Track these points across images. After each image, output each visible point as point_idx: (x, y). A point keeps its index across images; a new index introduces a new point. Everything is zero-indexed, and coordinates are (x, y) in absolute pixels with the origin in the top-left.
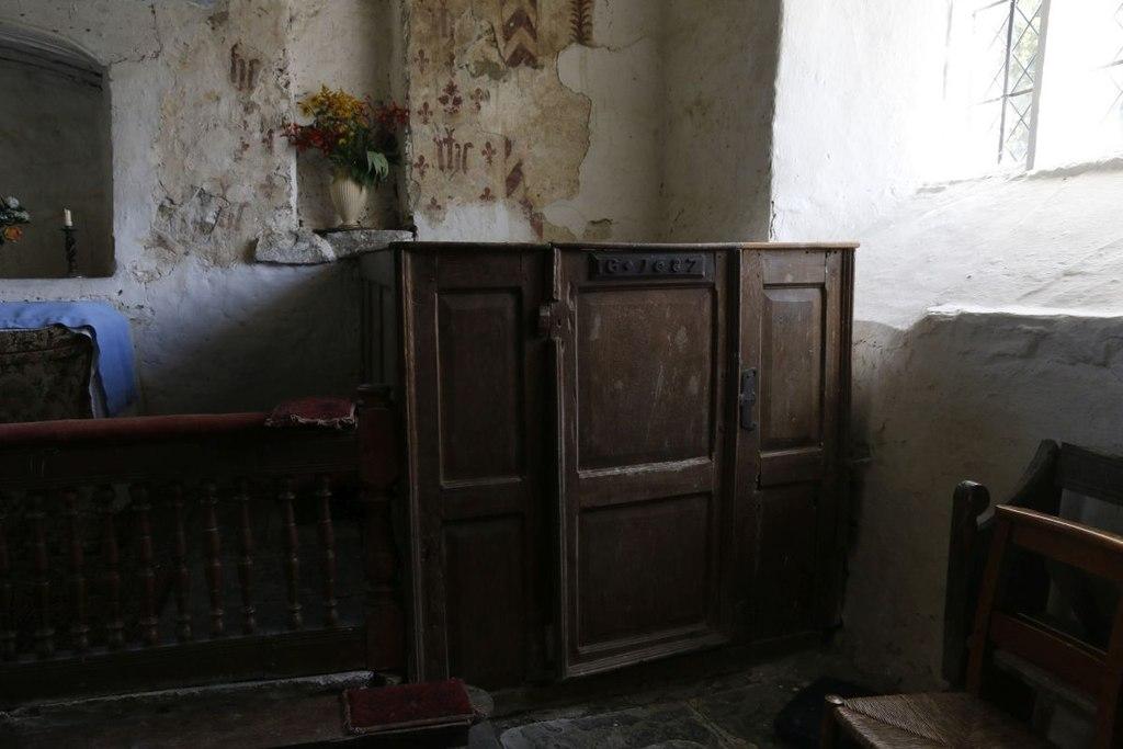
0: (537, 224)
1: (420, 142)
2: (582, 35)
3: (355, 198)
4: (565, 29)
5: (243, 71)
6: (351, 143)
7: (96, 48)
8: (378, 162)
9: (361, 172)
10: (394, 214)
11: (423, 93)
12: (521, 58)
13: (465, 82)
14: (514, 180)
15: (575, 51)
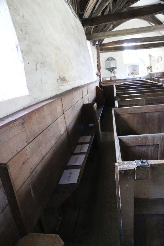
0: (159, 71)
1: (153, 67)
2: (161, 60)
3: (150, 70)
4: (161, 60)
5: (145, 65)
6: (150, 68)
7: (138, 65)
8: (151, 68)
9: (150, 69)
10: (151, 71)
11: (153, 65)
12: (158, 62)
13: (155, 64)
14: (158, 69)
15: (161, 62)
